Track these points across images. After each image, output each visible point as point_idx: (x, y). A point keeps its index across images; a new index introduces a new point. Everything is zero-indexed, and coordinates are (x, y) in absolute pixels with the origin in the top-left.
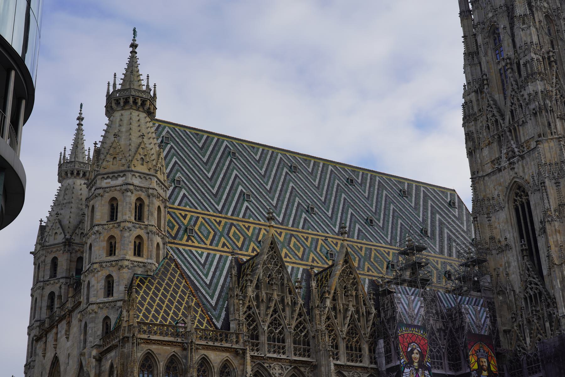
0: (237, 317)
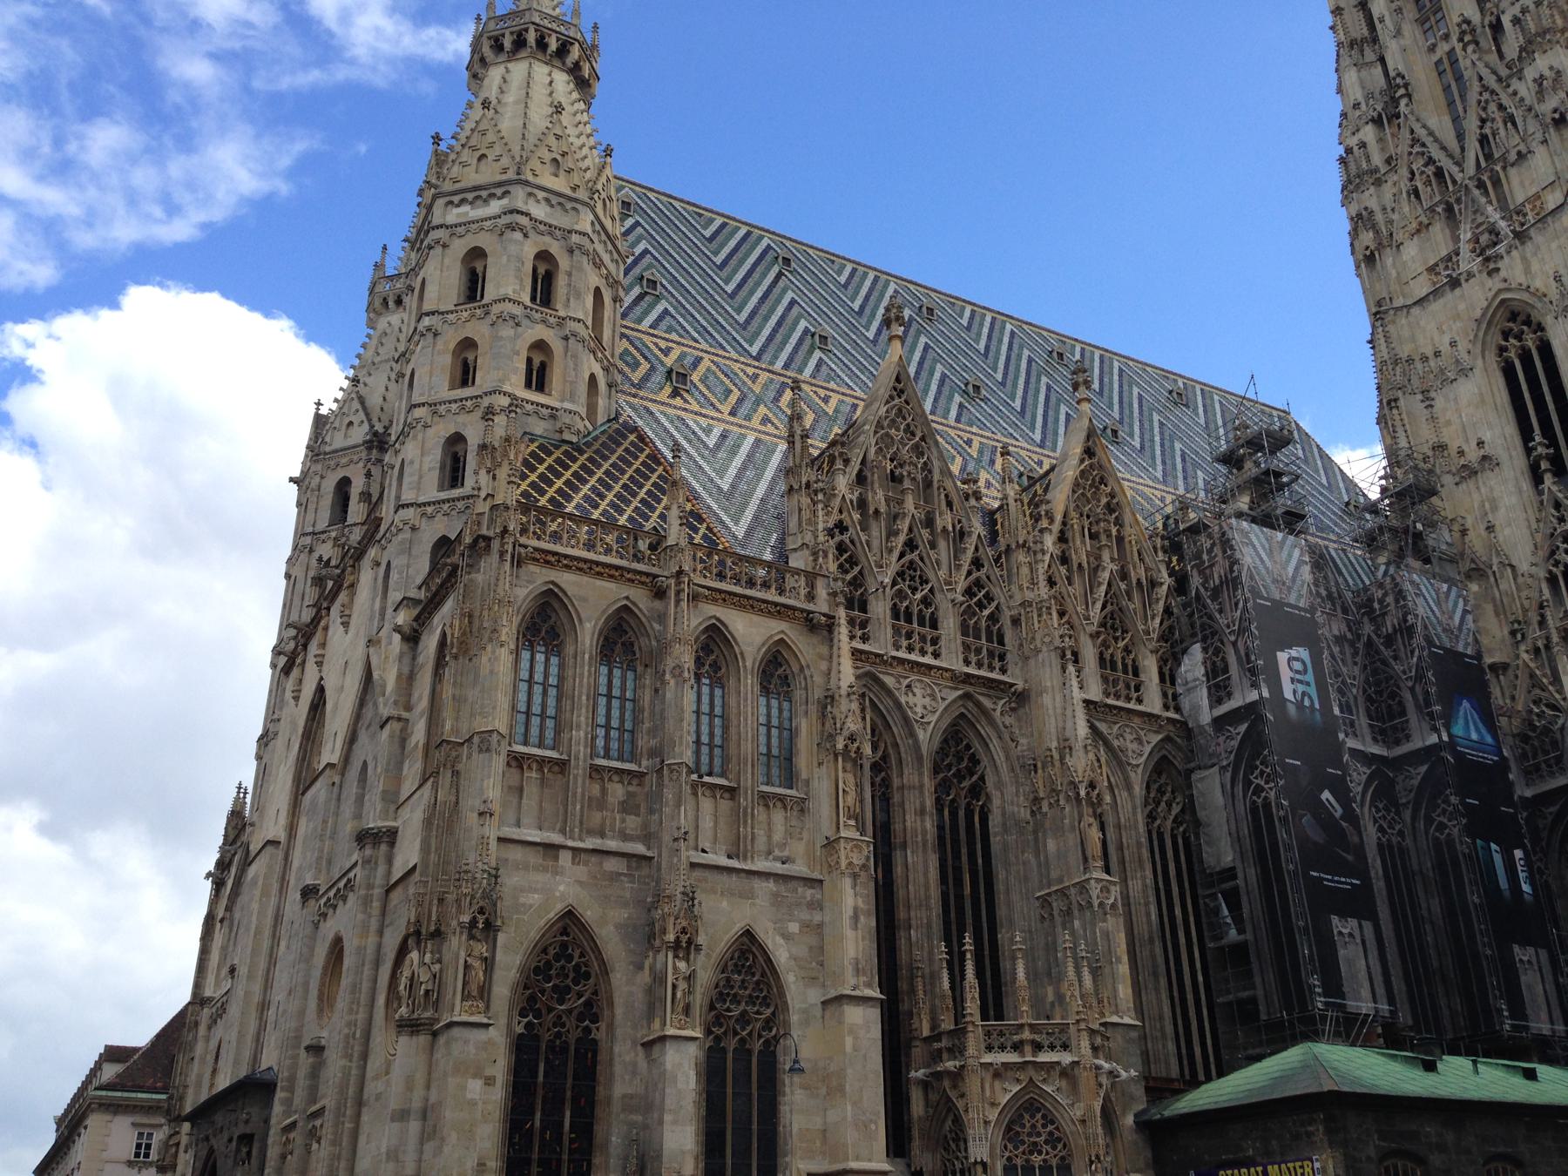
0: (808, 538)
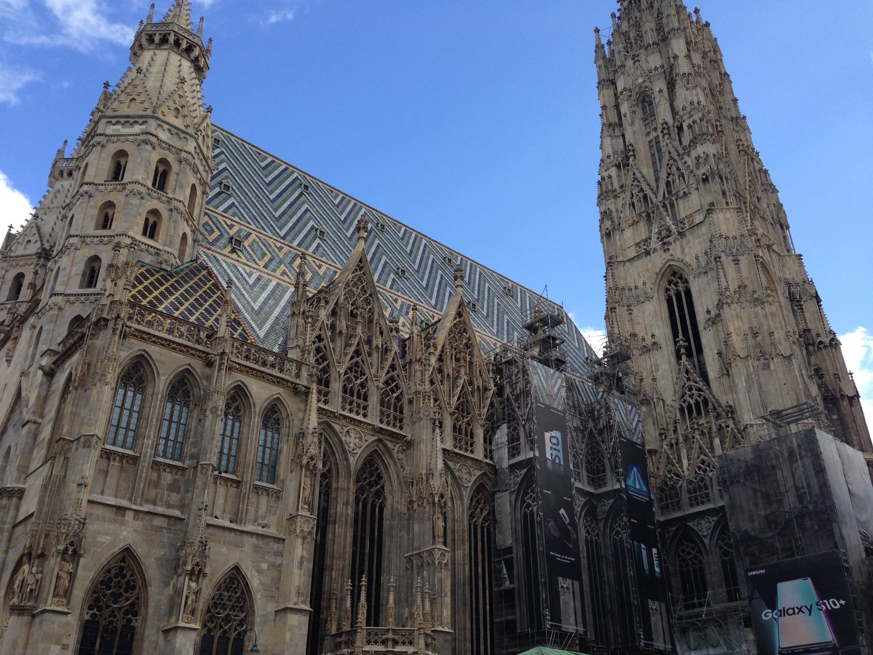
0: (300, 342)
